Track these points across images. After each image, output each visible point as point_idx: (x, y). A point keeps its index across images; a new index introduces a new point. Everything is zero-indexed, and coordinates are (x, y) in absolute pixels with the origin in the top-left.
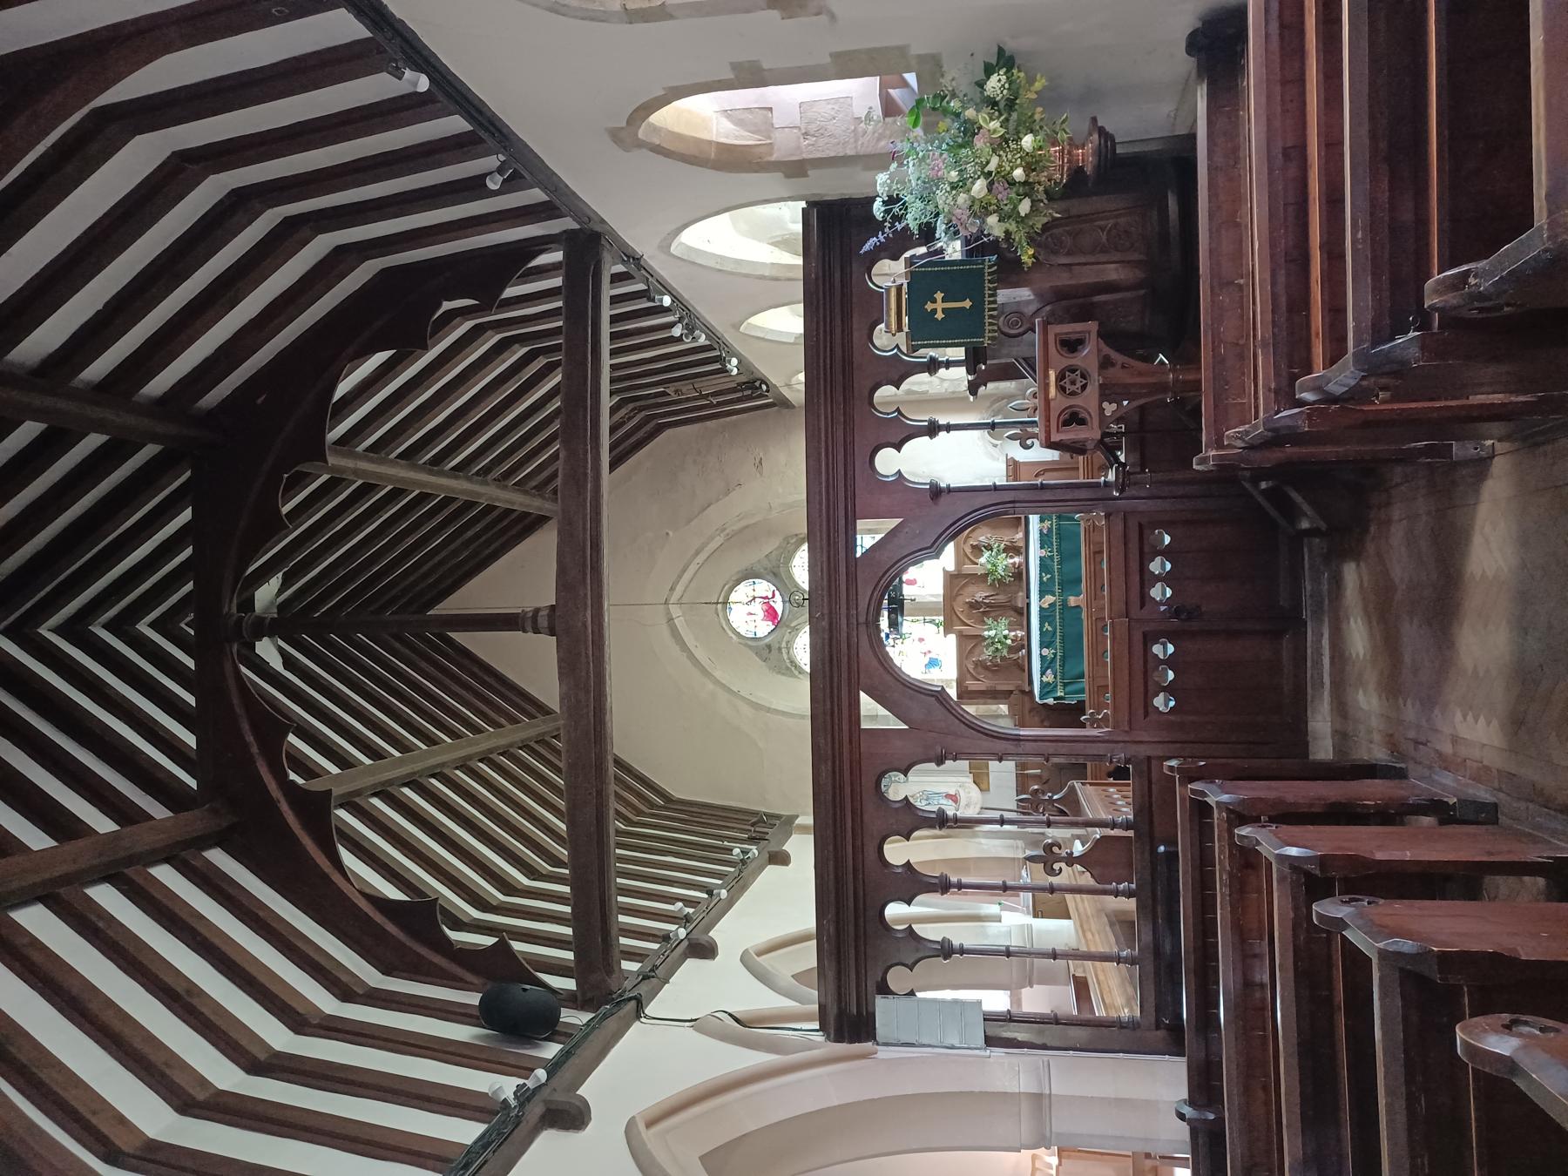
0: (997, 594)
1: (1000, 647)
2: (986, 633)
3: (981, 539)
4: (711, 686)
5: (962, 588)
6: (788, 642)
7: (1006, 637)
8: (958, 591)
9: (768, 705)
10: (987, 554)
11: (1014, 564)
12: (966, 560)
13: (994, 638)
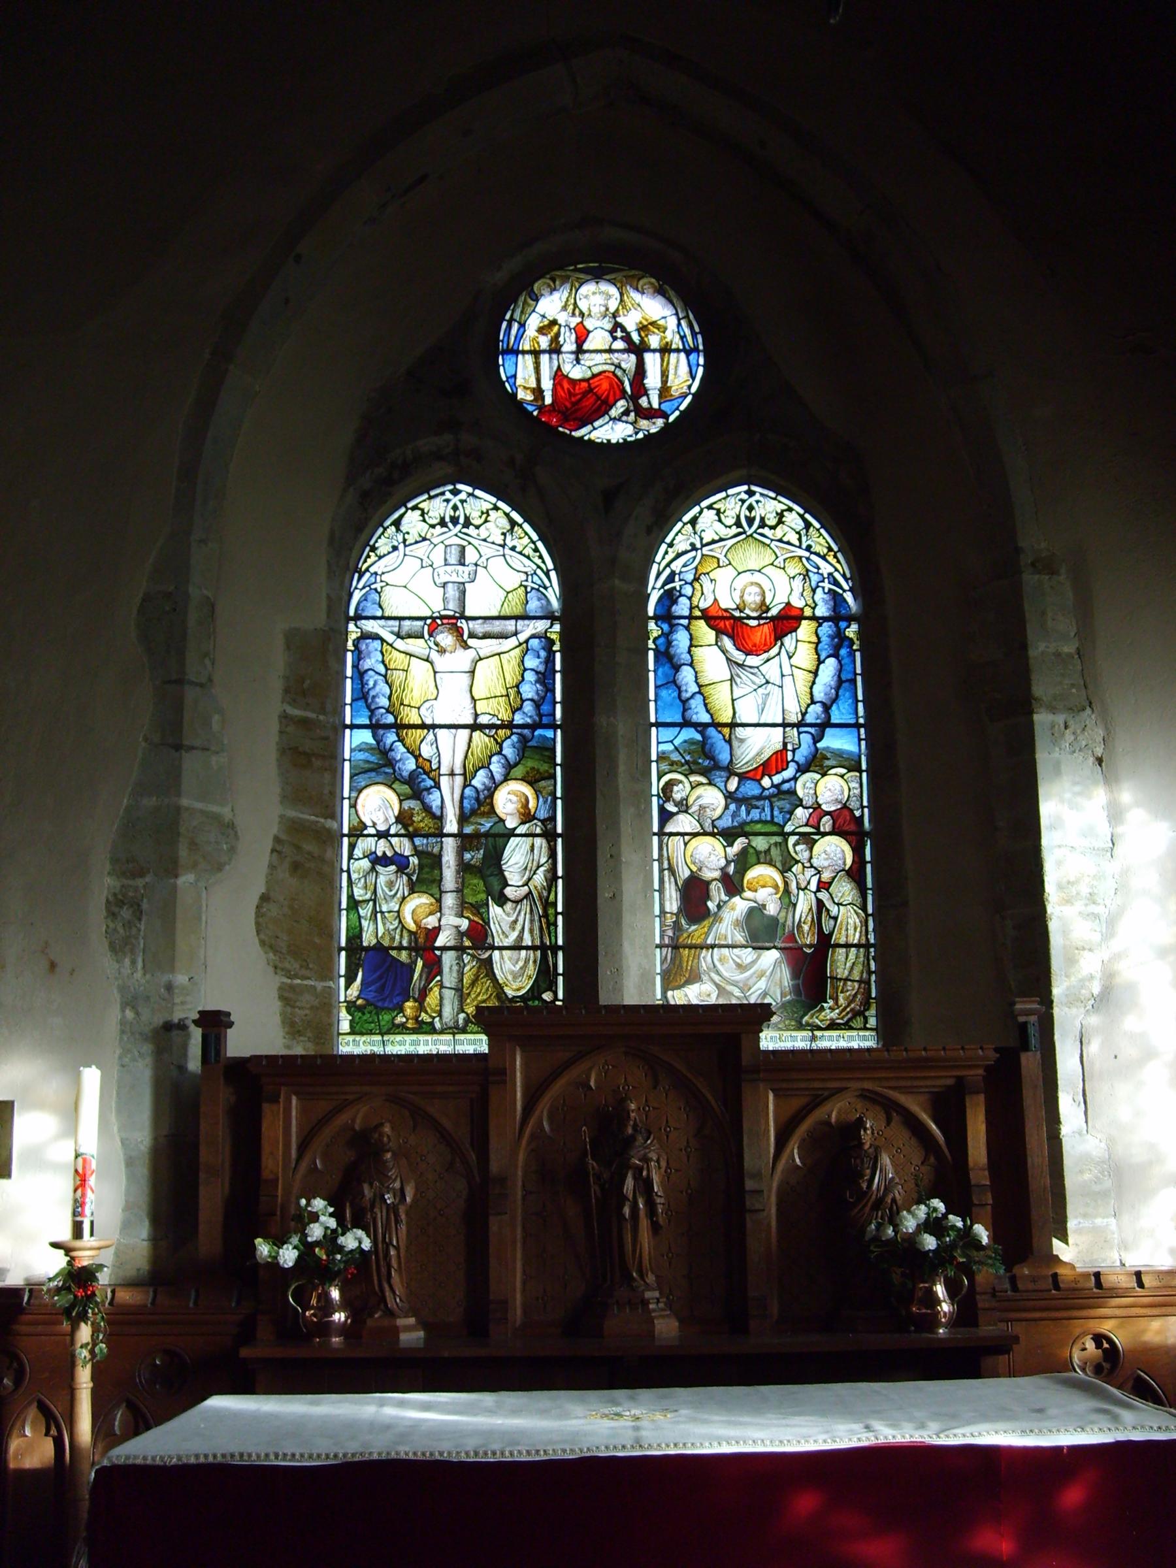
0: (655, 1228)
3: (886, 1160)
12: (796, 1103)
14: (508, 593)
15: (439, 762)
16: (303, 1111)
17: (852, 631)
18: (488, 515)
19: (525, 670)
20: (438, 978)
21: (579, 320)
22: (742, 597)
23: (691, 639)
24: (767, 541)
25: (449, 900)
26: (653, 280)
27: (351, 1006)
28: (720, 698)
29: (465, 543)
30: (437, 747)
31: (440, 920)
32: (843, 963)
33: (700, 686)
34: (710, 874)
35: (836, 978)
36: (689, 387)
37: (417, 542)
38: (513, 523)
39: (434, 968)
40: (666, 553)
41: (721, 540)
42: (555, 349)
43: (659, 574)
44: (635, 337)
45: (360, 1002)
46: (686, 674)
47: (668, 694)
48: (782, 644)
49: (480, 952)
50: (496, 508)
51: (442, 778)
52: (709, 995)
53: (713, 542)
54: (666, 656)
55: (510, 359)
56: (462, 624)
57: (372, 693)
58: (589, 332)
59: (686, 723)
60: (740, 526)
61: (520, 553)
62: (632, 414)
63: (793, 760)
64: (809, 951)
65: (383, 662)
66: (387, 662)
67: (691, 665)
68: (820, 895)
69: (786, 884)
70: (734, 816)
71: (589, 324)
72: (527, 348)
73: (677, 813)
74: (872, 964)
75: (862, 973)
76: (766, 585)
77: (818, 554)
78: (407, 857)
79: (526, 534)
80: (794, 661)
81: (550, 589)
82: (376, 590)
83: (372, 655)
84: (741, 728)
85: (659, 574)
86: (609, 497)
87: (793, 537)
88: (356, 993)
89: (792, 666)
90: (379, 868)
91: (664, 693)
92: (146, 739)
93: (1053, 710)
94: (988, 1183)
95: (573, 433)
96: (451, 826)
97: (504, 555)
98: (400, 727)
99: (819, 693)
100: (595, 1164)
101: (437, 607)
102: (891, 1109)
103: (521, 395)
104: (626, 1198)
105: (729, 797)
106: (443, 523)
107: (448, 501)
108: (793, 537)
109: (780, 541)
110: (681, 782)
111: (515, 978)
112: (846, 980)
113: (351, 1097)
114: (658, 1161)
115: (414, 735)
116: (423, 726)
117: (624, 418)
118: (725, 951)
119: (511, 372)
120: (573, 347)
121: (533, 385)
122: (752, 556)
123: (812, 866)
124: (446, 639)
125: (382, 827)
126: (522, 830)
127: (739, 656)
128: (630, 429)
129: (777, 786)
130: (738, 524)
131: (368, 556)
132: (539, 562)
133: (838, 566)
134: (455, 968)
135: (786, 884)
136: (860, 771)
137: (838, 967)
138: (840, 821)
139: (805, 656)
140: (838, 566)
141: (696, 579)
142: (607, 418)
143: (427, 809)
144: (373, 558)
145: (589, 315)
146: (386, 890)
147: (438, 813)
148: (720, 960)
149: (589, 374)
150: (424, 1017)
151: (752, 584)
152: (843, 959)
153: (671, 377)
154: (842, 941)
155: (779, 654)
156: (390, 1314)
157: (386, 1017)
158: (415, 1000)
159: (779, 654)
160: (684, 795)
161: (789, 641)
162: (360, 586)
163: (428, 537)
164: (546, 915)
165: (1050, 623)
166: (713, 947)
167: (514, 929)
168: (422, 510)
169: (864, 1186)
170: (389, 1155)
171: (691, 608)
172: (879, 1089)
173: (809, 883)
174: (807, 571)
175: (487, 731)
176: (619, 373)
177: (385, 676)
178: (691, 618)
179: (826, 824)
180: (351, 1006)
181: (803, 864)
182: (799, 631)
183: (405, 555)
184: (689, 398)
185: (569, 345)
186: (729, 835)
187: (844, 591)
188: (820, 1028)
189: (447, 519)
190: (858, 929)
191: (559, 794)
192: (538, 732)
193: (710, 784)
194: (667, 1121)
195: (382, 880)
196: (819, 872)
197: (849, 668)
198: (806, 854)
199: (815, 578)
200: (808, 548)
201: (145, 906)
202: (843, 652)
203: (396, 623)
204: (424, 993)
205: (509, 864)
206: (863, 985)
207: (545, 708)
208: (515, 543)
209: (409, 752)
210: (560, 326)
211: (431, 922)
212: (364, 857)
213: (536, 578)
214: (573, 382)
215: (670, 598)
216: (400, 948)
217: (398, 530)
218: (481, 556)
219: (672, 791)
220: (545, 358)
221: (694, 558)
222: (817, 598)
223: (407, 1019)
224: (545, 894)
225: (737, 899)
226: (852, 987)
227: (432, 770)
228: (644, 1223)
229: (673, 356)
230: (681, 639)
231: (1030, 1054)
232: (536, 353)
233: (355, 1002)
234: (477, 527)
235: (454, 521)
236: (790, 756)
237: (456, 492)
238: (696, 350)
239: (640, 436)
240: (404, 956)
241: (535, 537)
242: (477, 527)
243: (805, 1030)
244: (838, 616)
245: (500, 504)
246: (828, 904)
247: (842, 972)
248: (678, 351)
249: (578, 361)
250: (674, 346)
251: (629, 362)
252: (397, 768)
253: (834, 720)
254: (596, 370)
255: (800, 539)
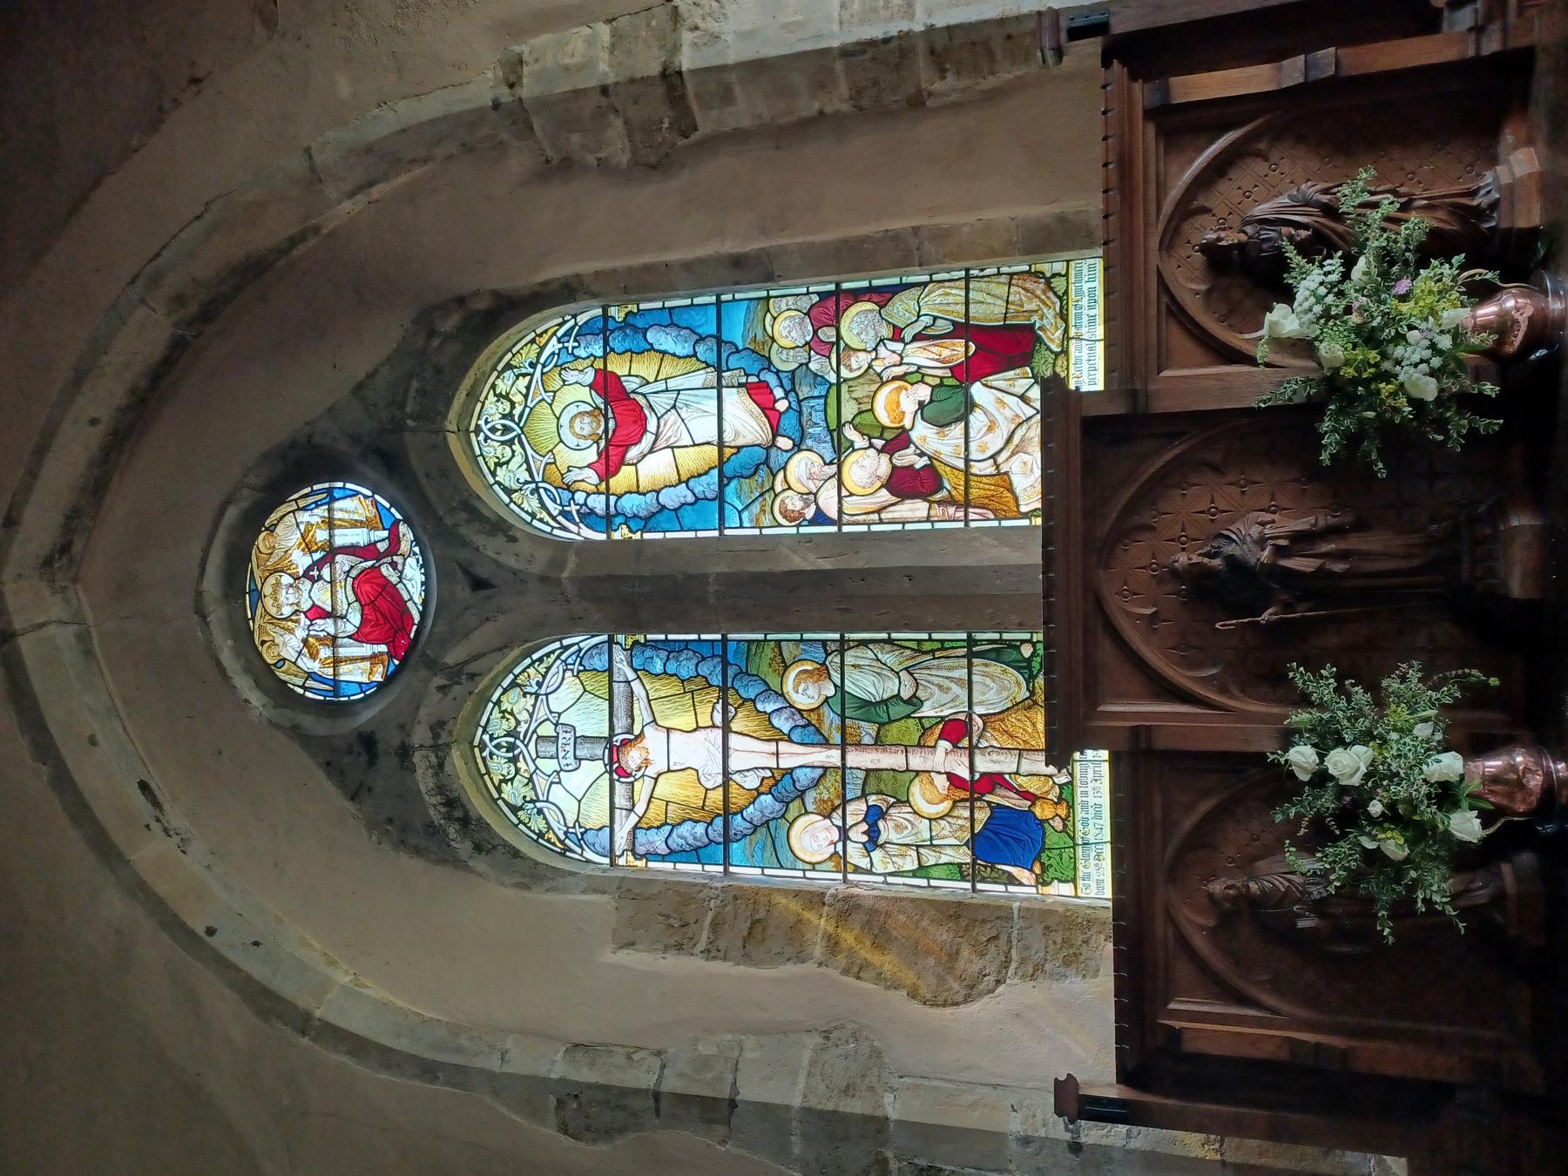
0: (1360, 526)
1: (1394, 845)
2: (1302, 756)
3: (1262, 210)
4: (116, 905)
5: (1150, 494)
6: (438, 727)
7: (1446, 795)
8: (1132, 507)
9: (304, 1002)
10: (1310, 281)
11: (1503, 327)
12: (1177, 338)
13: (1358, 796)
14: (585, 691)
15: (763, 768)
16: (1190, 993)
17: (617, 313)
18: (506, 711)
19: (665, 673)
20: (1007, 777)
21: (302, 616)
22: (585, 438)
23: (631, 492)
24: (527, 410)
25: (917, 761)
26: (261, 537)
27: (1041, 881)
28: (691, 460)
29: (535, 736)
30: (748, 770)
31: (939, 773)
32: (988, 309)
33: (680, 482)
34: (883, 466)
35: (1006, 313)
36: (366, 497)
37: (534, 788)
38: (513, 684)
39: (994, 781)
40: (541, 520)
41: (527, 461)
42: (333, 641)
43: (564, 529)
44: (317, 556)
45: (1037, 869)
46: (670, 498)
47: (688, 516)
48: (634, 392)
49: (975, 728)
50: (498, 702)
51: (781, 766)
52: (1024, 463)
53: (529, 470)
54: (646, 522)
55: (344, 688)
56: (617, 740)
57: (691, 841)
58: (314, 606)
59: (721, 498)
60: (513, 439)
61: (544, 677)
62: (395, 558)
63: (758, 376)
64: (973, 347)
65: (658, 828)
66: (658, 823)
67: (658, 492)
68: (908, 339)
69: (895, 378)
70: (820, 441)
71: (306, 606)
72: (331, 671)
73: (817, 504)
74: (987, 272)
75: (999, 283)
76: (573, 410)
77: (539, 355)
78: (868, 807)
79: (524, 671)
80: (651, 379)
81: (581, 645)
82: (582, 834)
83: (651, 839)
84: (725, 435)
85: (564, 529)
86: (479, 584)
87: (523, 382)
88: (1027, 873)
89: (656, 381)
90: (881, 841)
91: (687, 522)
92: (723, 1142)
93: (676, 48)
94: (1302, 57)
95: (416, 622)
96: (832, 757)
97: (547, 695)
98: (727, 812)
99: (683, 349)
100: (1270, 611)
101: (599, 767)
102: (1187, 209)
103: (378, 678)
104: (1320, 569)
105: (798, 447)
106: (514, 760)
107: (491, 754)
108: (523, 382)
109: (526, 396)
110: (782, 501)
111: (1005, 689)
112: (1007, 302)
113: (1171, 931)
114: (1263, 524)
115: (737, 797)
116: (726, 785)
117: (400, 568)
118: (973, 446)
119: (356, 688)
120: (330, 621)
121: (367, 665)
122: (544, 425)
123: (875, 349)
124: (632, 758)
125: (835, 835)
126: (837, 678)
127: (648, 439)
128: (411, 561)
129: (787, 393)
130: (510, 443)
131: (548, 841)
132: (553, 657)
133: (550, 332)
134: (994, 757)
135: (895, 378)
136: (768, 298)
137: (992, 313)
138: (823, 318)
139: (645, 367)
140: (550, 332)
141: (568, 488)
142: (400, 586)
143: (816, 783)
144: (551, 835)
145: (297, 604)
146: (906, 832)
147: (820, 771)
148: (984, 451)
149: (356, 605)
150: (1053, 796)
151: (571, 426)
152: (984, 306)
153: (356, 517)
154: (962, 309)
155: (644, 395)
156: (1499, 898)
157: (1053, 839)
158: (1033, 804)
159: (644, 395)
160: (797, 497)
161: (630, 384)
162: (579, 851)
163: (526, 775)
164: (933, 651)
165: (578, 59)
166: (967, 461)
167: (949, 689)
168: (501, 781)
169: (1304, 233)
170: (1253, 886)
171: (599, 493)
172: (1161, 227)
173: (894, 352)
174: (556, 366)
175: (731, 715)
176: (354, 573)
177: (673, 826)
178: (608, 494)
179: (828, 334)
180: (1041, 881)
181: (873, 360)
182: (619, 373)
183: (547, 801)
184: (376, 497)
185: (328, 626)
186: (841, 448)
187: (576, 324)
188: (1066, 330)
189: (511, 755)
190: (948, 290)
191: (797, 636)
192: (730, 658)
193: (784, 468)
194: (1203, 512)
195: (894, 837)
196: (881, 340)
197: (656, 318)
198: (862, 355)
199: (564, 358)
200: (532, 365)
201: (923, 1162)
202: (640, 323)
203: (617, 812)
204: (1026, 795)
205: (875, 693)
206: (1014, 282)
207: (706, 651)
208: (534, 683)
209: (753, 803)
210: (308, 635)
211: (942, 782)
212: (869, 856)
213: (570, 661)
214: (364, 620)
215: (587, 516)
216: (972, 819)
217: (521, 808)
218: (548, 719)
219: (793, 511)
220: (342, 652)
221: (545, 489)
222: (584, 355)
223: (1057, 815)
224: (908, 652)
225: (914, 435)
226: (1017, 294)
227: (773, 777)
228: (1354, 542)
229: (338, 515)
230: (630, 504)
231: (1113, 21)
232: (336, 662)
233: (1037, 875)
234: (518, 723)
235: (511, 747)
236: (753, 379)
237: (483, 747)
238: (330, 491)
239: (417, 550)
240: (982, 816)
241: (528, 661)
242: (518, 723)
243: (1067, 348)
244: (603, 329)
245: (494, 698)
246: (918, 328)
247: (1000, 308)
248: (330, 510)
249: (343, 617)
250: (326, 514)
251: (343, 562)
252: (772, 816)
253: (714, 331)
254: (352, 598)
255: (524, 375)
